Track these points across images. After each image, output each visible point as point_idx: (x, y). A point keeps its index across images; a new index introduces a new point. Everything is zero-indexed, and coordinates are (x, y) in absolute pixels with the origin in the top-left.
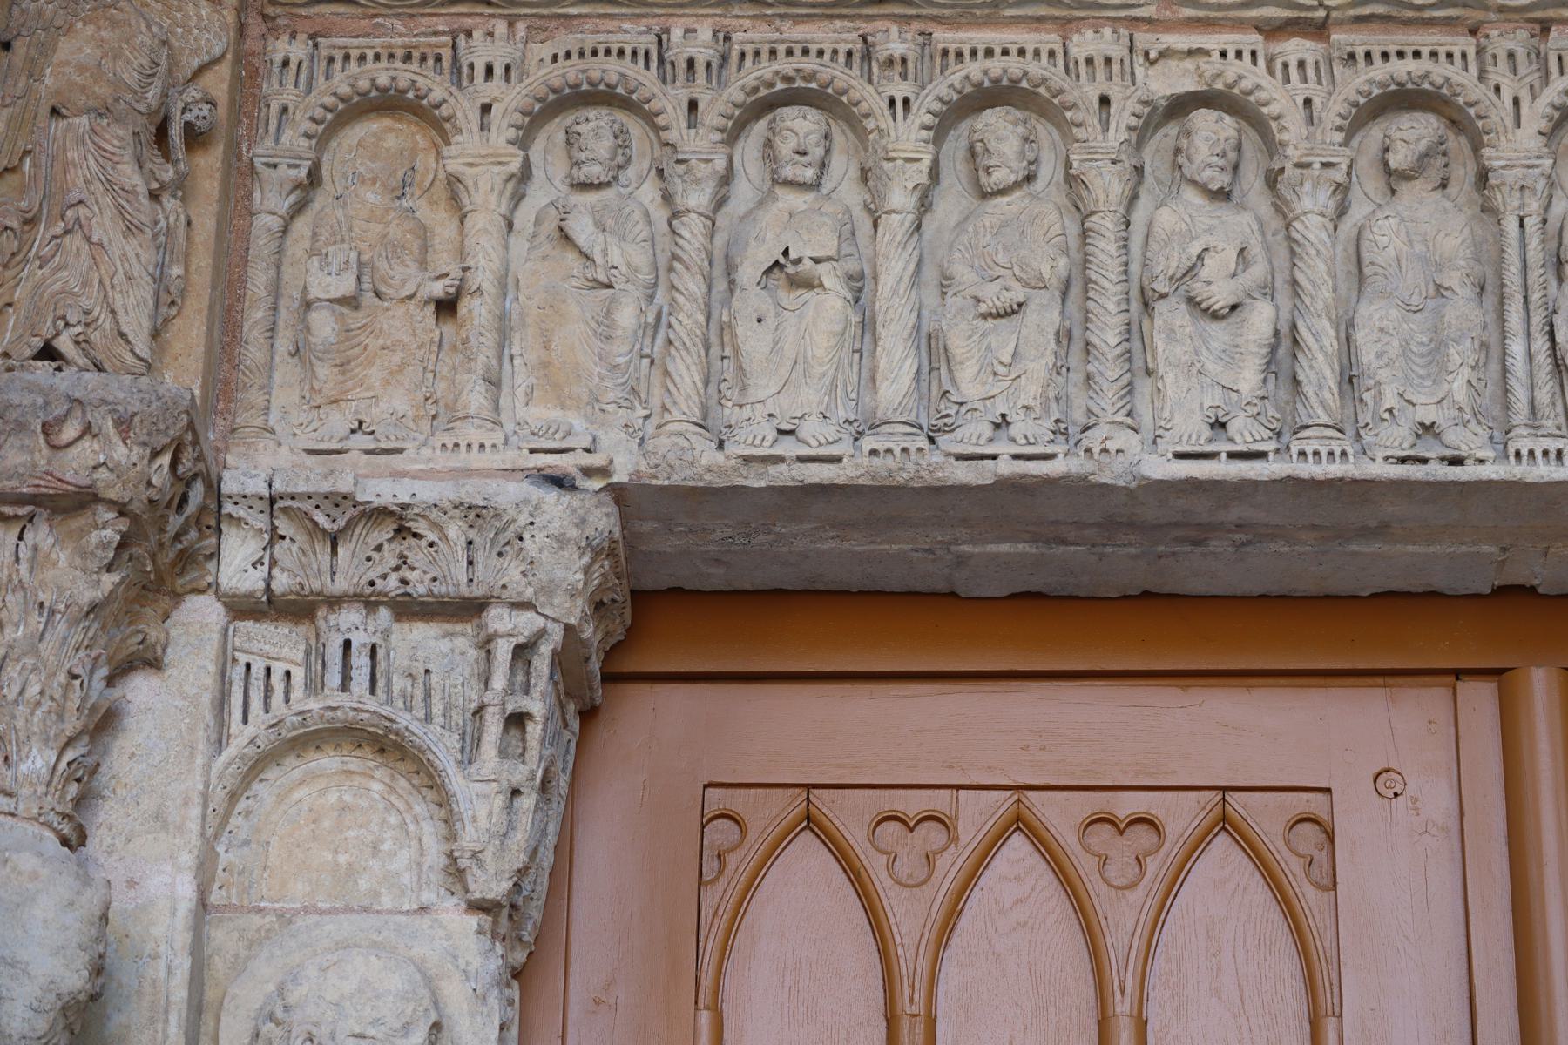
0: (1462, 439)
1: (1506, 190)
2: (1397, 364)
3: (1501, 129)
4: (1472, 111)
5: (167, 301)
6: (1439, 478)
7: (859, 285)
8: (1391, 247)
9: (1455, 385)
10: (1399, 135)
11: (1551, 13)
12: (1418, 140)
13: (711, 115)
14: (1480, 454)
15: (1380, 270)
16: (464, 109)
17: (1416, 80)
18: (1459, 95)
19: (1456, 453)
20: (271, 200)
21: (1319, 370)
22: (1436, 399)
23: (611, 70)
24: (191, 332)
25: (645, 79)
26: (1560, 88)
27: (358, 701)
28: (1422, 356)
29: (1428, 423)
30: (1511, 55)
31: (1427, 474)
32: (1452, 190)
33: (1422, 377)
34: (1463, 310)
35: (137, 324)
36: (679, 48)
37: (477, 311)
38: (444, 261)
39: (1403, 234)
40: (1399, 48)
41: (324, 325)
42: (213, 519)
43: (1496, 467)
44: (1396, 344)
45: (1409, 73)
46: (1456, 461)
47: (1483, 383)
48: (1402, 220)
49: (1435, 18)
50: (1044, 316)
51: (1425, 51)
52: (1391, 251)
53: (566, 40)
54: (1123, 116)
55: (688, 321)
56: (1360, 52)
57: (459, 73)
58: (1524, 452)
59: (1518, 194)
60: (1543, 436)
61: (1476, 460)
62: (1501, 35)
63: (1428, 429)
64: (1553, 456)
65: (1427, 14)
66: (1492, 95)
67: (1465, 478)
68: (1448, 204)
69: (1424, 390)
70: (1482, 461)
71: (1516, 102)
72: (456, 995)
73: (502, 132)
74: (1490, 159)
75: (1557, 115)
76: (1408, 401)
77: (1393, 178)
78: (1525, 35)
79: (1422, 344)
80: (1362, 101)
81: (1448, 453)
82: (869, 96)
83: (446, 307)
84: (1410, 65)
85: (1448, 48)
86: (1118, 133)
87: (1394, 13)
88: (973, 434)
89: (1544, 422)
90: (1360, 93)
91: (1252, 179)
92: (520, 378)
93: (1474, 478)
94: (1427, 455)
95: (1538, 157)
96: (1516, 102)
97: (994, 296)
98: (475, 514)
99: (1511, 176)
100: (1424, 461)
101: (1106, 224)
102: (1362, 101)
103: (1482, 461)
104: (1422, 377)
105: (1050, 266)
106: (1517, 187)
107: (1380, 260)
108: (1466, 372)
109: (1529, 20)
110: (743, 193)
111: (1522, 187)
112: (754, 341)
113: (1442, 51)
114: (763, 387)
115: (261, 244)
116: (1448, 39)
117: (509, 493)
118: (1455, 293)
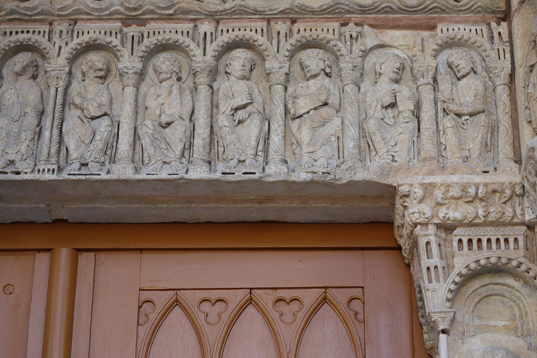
0: (19, 166)
1: (51, 78)
2: (4, 139)
3: (52, 57)
4: (44, 51)
6: (9, 179)
8: (11, 99)
9: (23, 147)
10: (17, 60)
11: (77, 17)
12: (23, 61)
14: (25, 170)
15: (6, 107)
17: (26, 41)
18: (41, 46)
19: (17, 170)
22: (16, 151)
26: (75, 43)
28: (14, 137)
29: (11, 160)
30: (61, 32)
31: (6, 177)
32: (39, 79)
33: (13, 144)
34: (31, 120)
39: (16, 95)
40: (22, 30)
43: (30, 175)
44: (5, 132)
45: (24, 38)
46: (18, 173)
47: (36, 147)
48: (16, 90)
49: (36, 19)
51: (31, 31)
52: (11, 101)
56: (8, 31)
58: (41, 170)
59: (56, 80)
60: (49, 164)
61: (25, 172)
62: (59, 25)
63: (12, 162)
64: (51, 171)
65: (33, 18)
66: (52, 46)
67: (19, 179)
68: (34, 84)
69: (12, 149)
70: (26, 173)
71: (60, 48)
74: (47, 68)
75: (74, 52)
76: (6, 152)
77: (19, 74)
78: (67, 24)
79: (15, 132)
80: (7, 48)
81: (15, 170)
84: (25, 36)
85: (39, 29)
87: (22, 18)
89: (51, 159)
90: (5, 45)
93: (22, 179)
94: (7, 171)
95: (64, 67)
96: (60, 48)
99: (53, 73)
100: (6, 173)
102: (7, 48)
103: (26, 173)
104: (13, 144)
106: (55, 77)
107: (7, 104)
108: (27, 142)
109: (69, 19)
111: (57, 78)
113: (37, 30)
116: (40, 26)
118: (29, 115)
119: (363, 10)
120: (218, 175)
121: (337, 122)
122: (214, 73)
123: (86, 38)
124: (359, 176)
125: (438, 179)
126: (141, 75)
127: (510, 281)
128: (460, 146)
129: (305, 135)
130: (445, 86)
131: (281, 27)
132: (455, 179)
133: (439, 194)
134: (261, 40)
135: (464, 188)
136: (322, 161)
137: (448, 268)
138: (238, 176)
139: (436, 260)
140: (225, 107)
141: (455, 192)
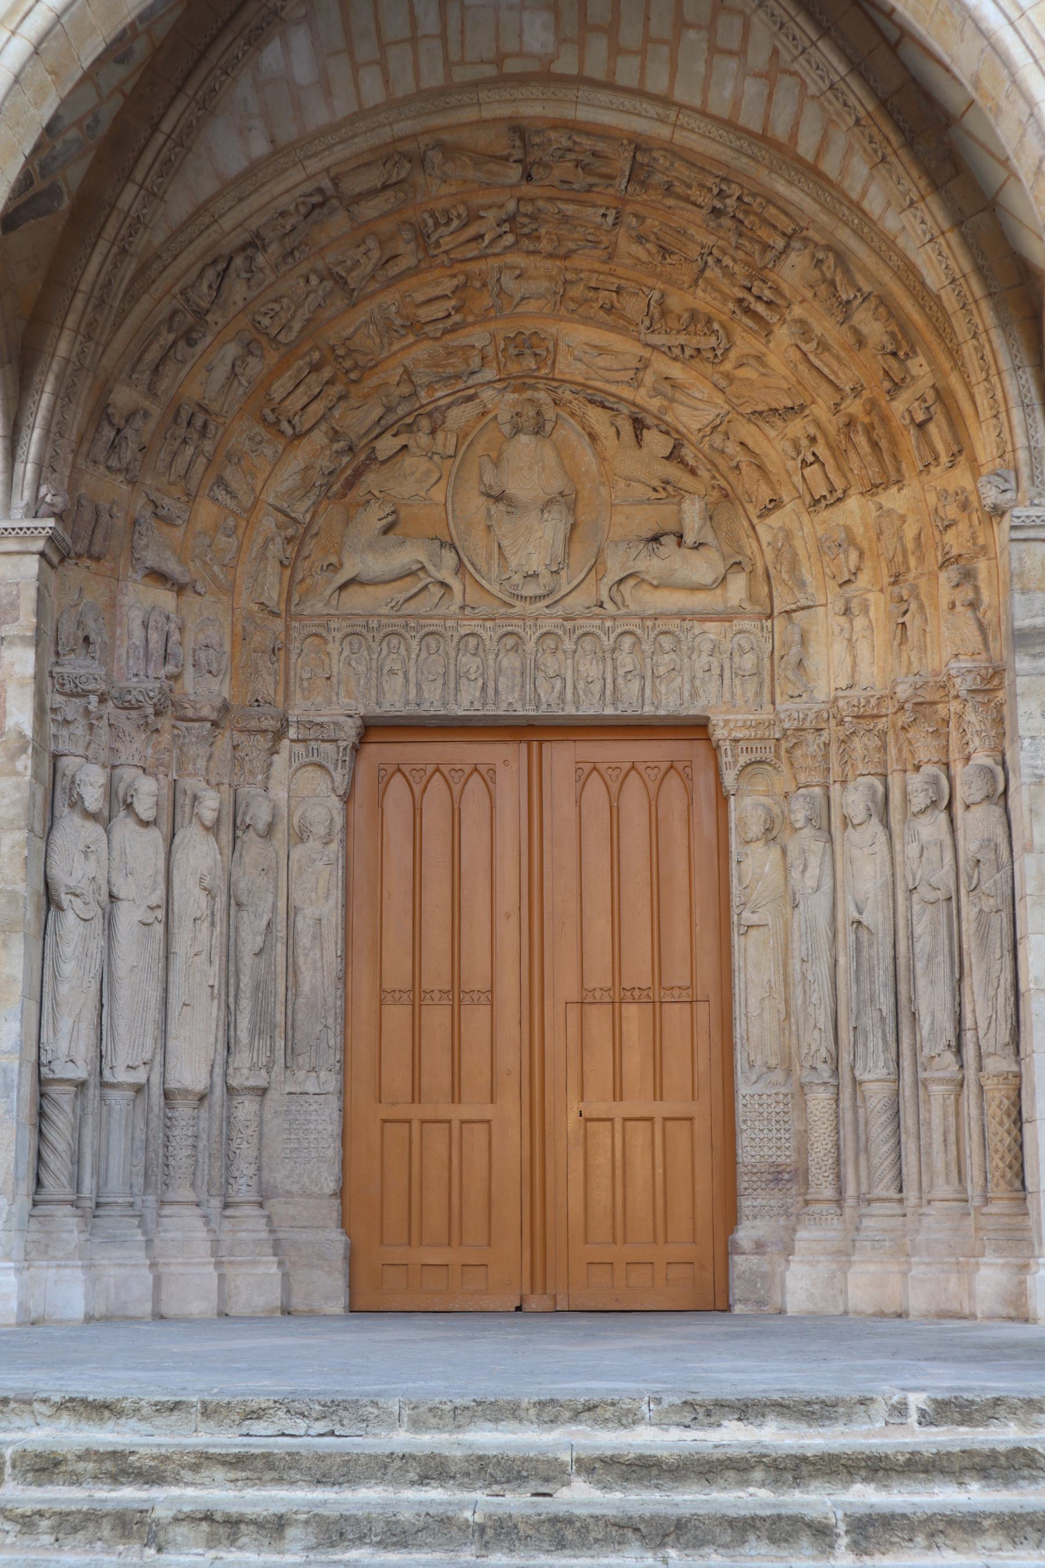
5: (276, 683)
7: (406, 673)
13: (377, 640)
16: (330, 639)
20: (293, 657)
21: (491, 691)
23: (358, 629)
24: (281, 688)
25: (364, 631)
27: (315, 759)
34: (518, 680)
35: (272, 692)
36: (371, 625)
37: (334, 680)
38: (327, 668)
41: (305, 684)
42: (288, 726)
50: (440, 681)
53: (349, 622)
54: (456, 639)
55: (374, 682)
57: (329, 630)
72: (335, 812)
73: (337, 644)
77: (508, 651)
82: (408, 636)
83: (328, 678)
86: (454, 644)
88: (426, 706)
91: (481, 652)
92: (342, 693)
97: (431, 677)
98: (335, 724)
101: (452, 661)
105: (441, 671)
110: (384, 653)
112: (386, 686)
114: (388, 696)
115: (292, 666)
117: (342, 719)
119: (693, 613)
120: (619, 712)
121: (679, 679)
122: (613, 651)
123: (544, 630)
124: (692, 712)
125: (731, 717)
126: (575, 652)
127: (767, 767)
128: (744, 694)
129: (663, 689)
130: (736, 659)
131: (649, 623)
132: (740, 717)
133: (732, 725)
134: (639, 632)
135: (745, 722)
136: (672, 704)
137: (736, 762)
138: (629, 713)
139: (730, 759)
140: (621, 672)
141: (740, 724)
